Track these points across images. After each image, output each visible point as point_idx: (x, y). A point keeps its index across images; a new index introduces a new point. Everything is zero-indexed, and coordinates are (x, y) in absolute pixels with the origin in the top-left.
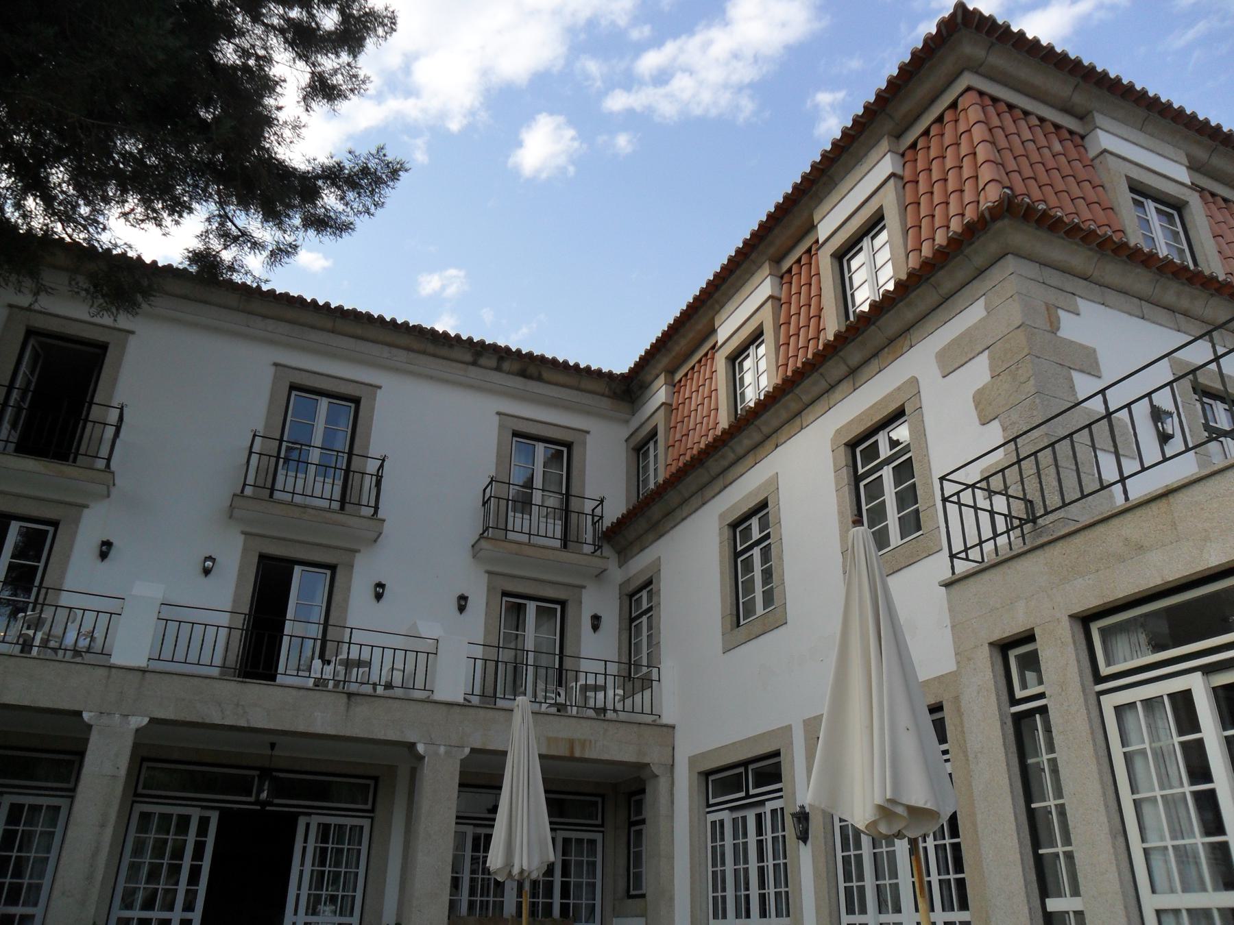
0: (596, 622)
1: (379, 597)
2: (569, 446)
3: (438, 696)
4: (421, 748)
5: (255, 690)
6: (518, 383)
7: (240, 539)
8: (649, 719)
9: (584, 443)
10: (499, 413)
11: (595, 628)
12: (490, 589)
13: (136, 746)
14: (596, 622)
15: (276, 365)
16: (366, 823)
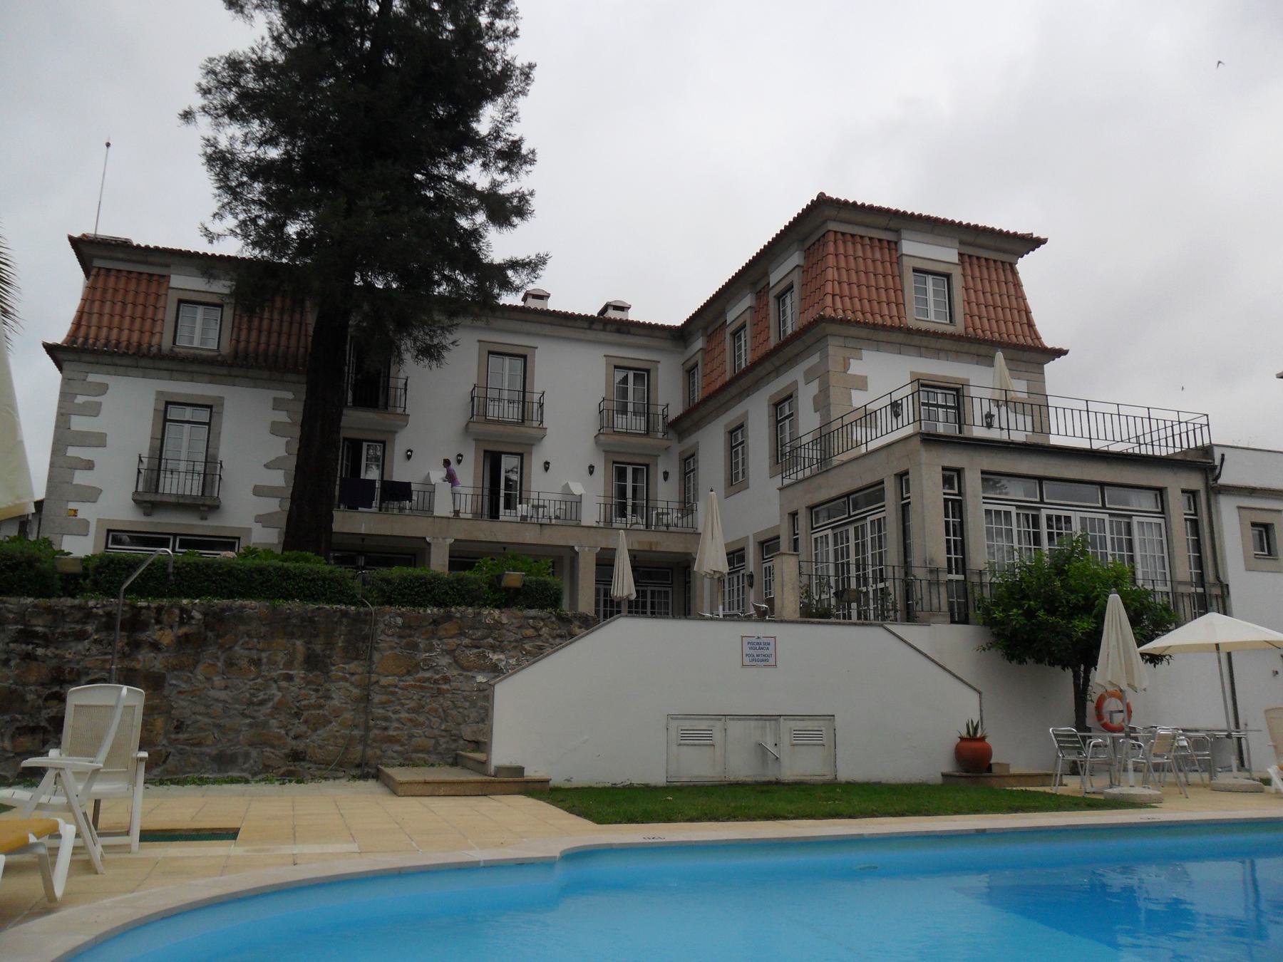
0: (666, 476)
1: (547, 469)
2: (648, 371)
3: (583, 523)
4: (576, 548)
5: (495, 525)
7: (474, 443)
8: (691, 530)
9: (657, 369)
10: (605, 356)
11: (666, 479)
14: (666, 476)
15: (479, 341)
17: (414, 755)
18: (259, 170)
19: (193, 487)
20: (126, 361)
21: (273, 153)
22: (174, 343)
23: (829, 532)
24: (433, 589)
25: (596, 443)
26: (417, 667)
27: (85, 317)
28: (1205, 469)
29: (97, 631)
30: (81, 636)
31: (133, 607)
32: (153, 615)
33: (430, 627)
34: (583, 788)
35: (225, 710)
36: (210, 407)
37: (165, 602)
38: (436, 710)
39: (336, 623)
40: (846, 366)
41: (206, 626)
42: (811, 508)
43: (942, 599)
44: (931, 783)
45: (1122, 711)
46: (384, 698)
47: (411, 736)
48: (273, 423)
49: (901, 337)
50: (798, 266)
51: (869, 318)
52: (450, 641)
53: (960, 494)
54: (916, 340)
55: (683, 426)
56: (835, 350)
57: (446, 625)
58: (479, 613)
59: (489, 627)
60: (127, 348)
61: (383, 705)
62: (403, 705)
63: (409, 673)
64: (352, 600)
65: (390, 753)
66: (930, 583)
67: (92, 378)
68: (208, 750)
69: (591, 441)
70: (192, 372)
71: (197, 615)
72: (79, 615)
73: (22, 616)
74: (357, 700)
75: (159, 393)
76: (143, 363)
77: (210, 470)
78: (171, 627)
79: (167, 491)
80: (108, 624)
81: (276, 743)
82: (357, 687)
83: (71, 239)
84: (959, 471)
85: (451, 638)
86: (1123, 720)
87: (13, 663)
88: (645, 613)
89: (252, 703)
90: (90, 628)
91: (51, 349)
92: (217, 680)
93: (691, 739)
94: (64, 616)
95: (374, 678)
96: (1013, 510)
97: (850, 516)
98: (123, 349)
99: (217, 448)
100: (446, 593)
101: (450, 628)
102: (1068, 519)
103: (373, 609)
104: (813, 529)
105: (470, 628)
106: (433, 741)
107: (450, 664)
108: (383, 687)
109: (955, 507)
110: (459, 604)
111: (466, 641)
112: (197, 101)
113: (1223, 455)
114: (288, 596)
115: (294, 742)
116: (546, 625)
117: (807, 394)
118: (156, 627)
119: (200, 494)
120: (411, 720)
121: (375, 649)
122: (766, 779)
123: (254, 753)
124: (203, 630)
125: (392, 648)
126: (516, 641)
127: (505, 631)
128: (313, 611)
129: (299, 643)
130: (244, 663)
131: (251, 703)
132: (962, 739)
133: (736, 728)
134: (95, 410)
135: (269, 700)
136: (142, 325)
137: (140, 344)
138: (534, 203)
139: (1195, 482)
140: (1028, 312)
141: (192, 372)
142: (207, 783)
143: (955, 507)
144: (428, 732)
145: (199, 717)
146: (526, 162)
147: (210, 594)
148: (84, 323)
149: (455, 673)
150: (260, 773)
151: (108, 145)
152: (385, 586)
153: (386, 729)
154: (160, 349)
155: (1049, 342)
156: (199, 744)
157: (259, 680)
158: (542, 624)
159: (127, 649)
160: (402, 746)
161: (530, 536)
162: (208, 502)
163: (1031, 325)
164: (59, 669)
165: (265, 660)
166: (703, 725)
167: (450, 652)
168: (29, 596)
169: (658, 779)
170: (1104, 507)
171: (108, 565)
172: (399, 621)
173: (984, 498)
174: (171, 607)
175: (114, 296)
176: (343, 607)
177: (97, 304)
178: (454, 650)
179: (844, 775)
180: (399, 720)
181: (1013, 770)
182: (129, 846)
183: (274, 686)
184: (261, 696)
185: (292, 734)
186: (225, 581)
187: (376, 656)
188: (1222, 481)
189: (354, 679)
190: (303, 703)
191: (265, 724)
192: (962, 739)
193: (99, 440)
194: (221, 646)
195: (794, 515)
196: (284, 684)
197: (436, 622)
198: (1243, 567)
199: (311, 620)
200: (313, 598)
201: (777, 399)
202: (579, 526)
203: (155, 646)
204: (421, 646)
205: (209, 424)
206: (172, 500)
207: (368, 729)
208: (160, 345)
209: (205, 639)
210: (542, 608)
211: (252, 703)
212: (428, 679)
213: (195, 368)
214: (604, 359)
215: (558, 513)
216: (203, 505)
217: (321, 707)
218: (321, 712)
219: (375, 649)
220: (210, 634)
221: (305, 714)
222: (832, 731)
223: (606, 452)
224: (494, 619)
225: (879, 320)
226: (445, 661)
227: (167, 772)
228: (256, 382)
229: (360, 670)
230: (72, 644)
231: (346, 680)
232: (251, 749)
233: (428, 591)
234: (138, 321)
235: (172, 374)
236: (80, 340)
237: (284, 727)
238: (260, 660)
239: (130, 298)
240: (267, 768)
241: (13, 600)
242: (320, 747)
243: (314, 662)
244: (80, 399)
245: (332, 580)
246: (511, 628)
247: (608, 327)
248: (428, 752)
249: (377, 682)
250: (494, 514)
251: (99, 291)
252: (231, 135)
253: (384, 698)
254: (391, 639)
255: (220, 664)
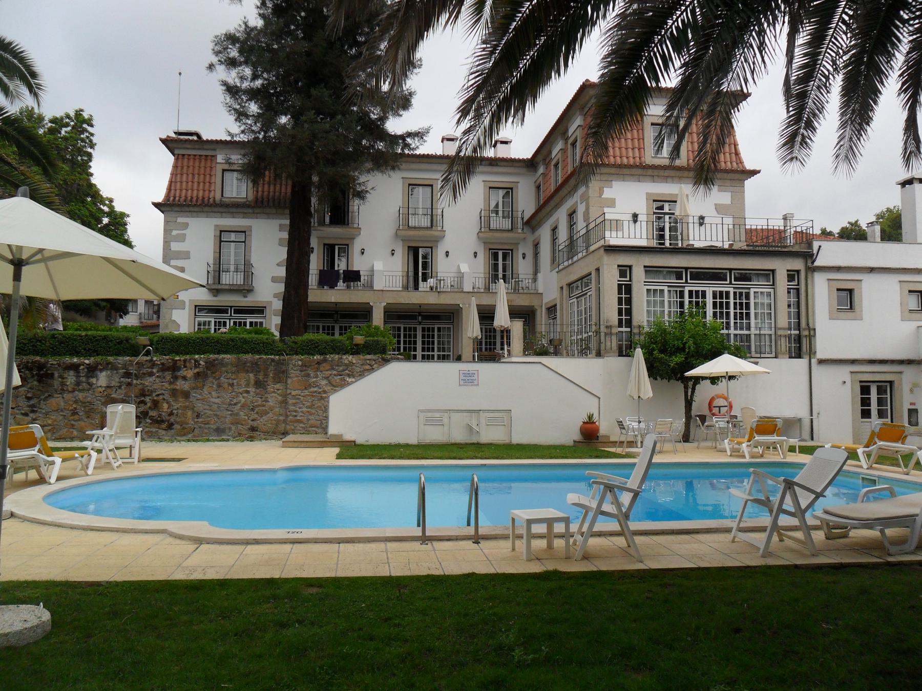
1: (447, 256)
2: (512, 189)
3: (465, 290)
4: (461, 306)
6: (489, 169)
7: (401, 242)
8: (535, 292)
9: (517, 187)
10: (483, 181)
11: (524, 258)
12: (485, 248)
13: (385, 312)
15: (403, 178)
16: (451, 326)
17: (310, 429)
18: (253, 94)
19: (238, 279)
20: (196, 209)
21: (258, 83)
22: (222, 196)
23: (575, 300)
24: (318, 346)
25: (478, 238)
26: (310, 386)
27: (173, 184)
28: (806, 257)
29: (158, 372)
30: (151, 374)
31: (173, 360)
32: (183, 363)
33: (316, 366)
34: (374, 445)
35: (219, 407)
36: (245, 232)
37: (188, 357)
38: (321, 407)
39: (269, 365)
40: (601, 192)
41: (207, 368)
42: (569, 285)
43: (614, 343)
44: (567, 445)
45: (726, 406)
46: (294, 401)
47: (308, 420)
48: (280, 239)
49: (639, 171)
50: (579, 126)
51: (619, 160)
52: (327, 372)
53: (630, 280)
54: (650, 172)
55: (532, 223)
56: (594, 184)
57: (324, 365)
58: (341, 358)
59: (346, 365)
60: (197, 201)
61: (294, 404)
62: (304, 404)
63: (306, 389)
64: (279, 353)
65: (298, 428)
66: (606, 334)
67: (180, 220)
68: (212, 426)
69: (476, 235)
70: (233, 213)
71: (202, 363)
72: (149, 365)
73: (125, 366)
74: (281, 402)
75: (216, 226)
76: (206, 209)
77: (247, 270)
78: (191, 369)
79: (224, 283)
80: (164, 368)
81: (244, 423)
82: (281, 396)
83: (161, 140)
84: (630, 267)
85: (327, 371)
86: (727, 412)
87: (123, 387)
88: (415, 357)
89: (231, 404)
90: (155, 370)
91: (157, 205)
92: (214, 394)
93: (430, 422)
94: (143, 365)
95: (289, 391)
96: (666, 289)
97: (582, 292)
98: (194, 202)
99: (250, 256)
100: (325, 348)
101: (325, 366)
102: (704, 293)
103: (286, 357)
104: (570, 297)
105: (338, 366)
106: (320, 422)
107: (327, 384)
108: (293, 396)
109: (626, 290)
110: (332, 354)
111: (335, 372)
112: (214, 59)
113: (820, 247)
114: (246, 352)
115: (252, 423)
116: (376, 363)
117: (581, 209)
118: (185, 369)
119: (242, 283)
120: (308, 412)
121: (289, 377)
122: (472, 442)
123: (233, 428)
124: (205, 370)
125: (297, 376)
126: (360, 372)
127: (354, 367)
128: (257, 359)
129: (251, 375)
130: (226, 385)
131: (230, 404)
132: (584, 423)
133: (456, 417)
134: (181, 239)
135: (239, 402)
136: (204, 186)
137: (203, 198)
138: (414, 101)
139: (797, 264)
140: (736, 145)
141: (233, 213)
142: (211, 441)
143: (626, 290)
144: (317, 418)
145: (207, 411)
146: (415, 67)
147: (209, 352)
148: (173, 188)
149: (329, 388)
150: (237, 437)
151: (180, 74)
152: (293, 345)
153: (296, 416)
154: (214, 201)
155: (749, 166)
156: (208, 424)
157: (234, 393)
158: (374, 362)
159: (172, 380)
160: (304, 424)
161: (432, 299)
162: (246, 288)
163: (737, 154)
164: (143, 390)
165: (235, 384)
166: (438, 415)
167: (327, 378)
168: (128, 356)
169: (413, 441)
170: (731, 283)
171: (161, 341)
172: (300, 363)
173: (645, 282)
174: (190, 359)
175: (187, 171)
176: (273, 357)
177: (179, 176)
178: (328, 377)
179: (516, 440)
180: (302, 412)
181: (612, 439)
182: (134, 462)
183: (241, 396)
184: (235, 401)
185: (251, 418)
186: (216, 346)
187: (289, 381)
188: (817, 264)
189: (279, 392)
190: (255, 404)
191: (237, 414)
192: (584, 423)
193: (186, 255)
194: (214, 378)
195: (562, 288)
196: (245, 395)
197: (319, 363)
198: (827, 316)
199: (256, 364)
200: (259, 353)
201: (570, 212)
202: (462, 292)
203: (184, 378)
204: (312, 375)
205: (244, 242)
206: (227, 287)
207: (287, 416)
208: (214, 198)
209: (207, 375)
210: (375, 354)
211: (231, 404)
212: (316, 392)
213: (234, 210)
214: (483, 183)
215: (452, 284)
216: (244, 290)
217: (264, 406)
218: (264, 408)
219: (289, 377)
220: (209, 372)
221: (257, 409)
222: (510, 418)
223: (484, 243)
224: (349, 361)
225: (625, 161)
226: (324, 382)
227: (194, 436)
228: (269, 216)
229: (281, 388)
230: (148, 378)
231: (274, 392)
232: (232, 426)
233: (316, 347)
234: (202, 184)
235: (222, 214)
236: (172, 198)
237: (247, 415)
238: (233, 384)
239: (196, 171)
240: (240, 434)
241: (121, 358)
242: (264, 425)
243: (258, 384)
244: (174, 233)
245: (267, 343)
246: (358, 365)
247: (484, 163)
248: (317, 427)
249: (290, 393)
250: (416, 287)
251: (179, 168)
252: (232, 77)
253: (294, 401)
254: (296, 372)
255: (214, 386)
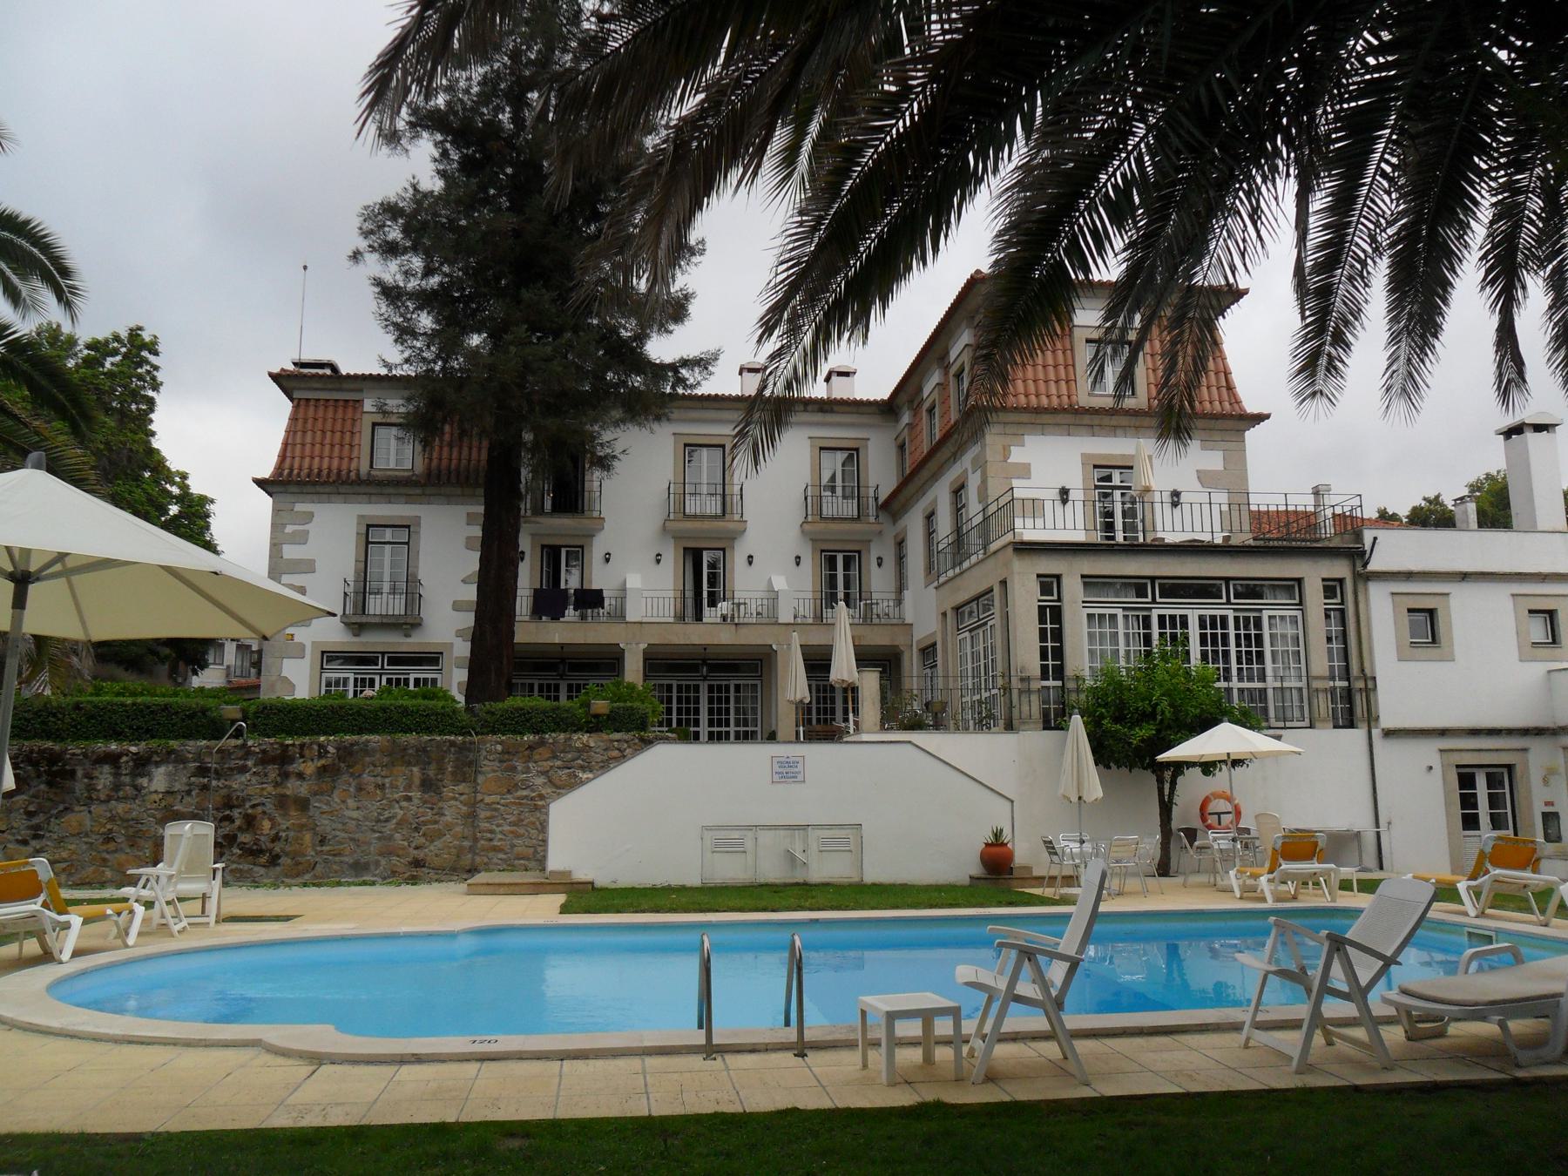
0: (880, 562)
1: (750, 563)
2: (857, 450)
3: (780, 621)
4: (774, 647)
6: (819, 417)
7: (672, 541)
8: (900, 622)
9: (866, 447)
11: (880, 565)
12: (814, 550)
13: (645, 660)
14: (880, 562)
15: (674, 434)
16: (759, 682)
18: (425, 299)
19: (397, 606)
20: (328, 489)
21: (434, 281)
22: (371, 467)
23: (967, 634)
24: (531, 718)
25: (803, 532)
27: (289, 448)
29: (255, 765)
30: (243, 770)
31: (282, 745)
32: (297, 750)
33: (527, 753)
35: (358, 826)
36: (408, 527)
37: (307, 739)
38: (534, 823)
39: (445, 752)
40: (1006, 457)
42: (957, 609)
44: (958, 884)
45: (1229, 813)
46: (488, 814)
47: (513, 846)
48: (468, 538)
50: (966, 345)
51: (1034, 401)
53: (1059, 599)
54: (1086, 419)
55: (893, 507)
59: (579, 750)
60: (329, 475)
61: (489, 819)
62: (505, 819)
63: (509, 792)
64: (463, 731)
65: (495, 860)
66: (1021, 692)
67: (299, 507)
70: (389, 494)
71: (330, 749)
72: (241, 753)
73: (198, 756)
75: (361, 517)
76: (342, 489)
77: (411, 590)
78: (312, 760)
79: (371, 612)
80: (265, 759)
81: (401, 852)
82: (465, 805)
83: (271, 375)
84: (1058, 577)
85: (546, 760)
86: (1231, 822)
87: (193, 793)
88: (696, 737)
90: (250, 763)
91: (261, 483)
92: (351, 803)
94: (230, 754)
95: (479, 797)
96: (1120, 613)
97: (979, 620)
98: (324, 478)
99: (417, 567)
100: (543, 721)
101: (543, 752)
102: (1184, 619)
103: (476, 738)
104: (959, 630)
106: (532, 850)
108: (488, 804)
109: (1051, 615)
110: (554, 731)
111: (559, 763)
112: (362, 244)
113: (1375, 539)
114: (407, 730)
115: (415, 852)
116: (629, 747)
117: (974, 482)
118: (302, 760)
119: (403, 613)
120: (512, 832)
122: (795, 881)
123: (383, 862)
124: (337, 761)
125: (494, 771)
126: (602, 761)
129: (415, 769)
130: (371, 788)
131: (378, 821)
132: (987, 845)
133: (766, 837)
134: (301, 538)
135: (393, 817)
136: (341, 451)
137: (339, 471)
138: (692, 308)
139: (1339, 569)
140: (1227, 373)
141: (389, 494)
143: (1051, 615)
145: (338, 833)
146: (693, 254)
148: (288, 454)
149: (549, 791)
150: (389, 877)
151: (305, 268)
152: (488, 718)
153: (491, 840)
154: (358, 474)
155: (1251, 407)
156: (339, 854)
157: (384, 802)
158: (626, 745)
159: (279, 779)
160: (506, 854)
161: (726, 637)
162: (409, 621)
163: (1230, 388)
164: (229, 797)
165: (387, 785)
166: (736, 835)
167: (545, 773)
168: (204, 739)
169: (694, 880)
170: (1228, 602)
171: (262, 712)
172: (499, 748)
173: (1083, 602)
174: (311, 744)
175: (313, 426)
177: (299, 434)
178: (548, 771)
179: (871, 876)
181: (1036, 873)
182: (208, 923)
183: (397, 806)
184: (387, 814)
185: (413, 845)
186: (356, 720)
187: (480, 779)
188: (1372, 567)
189: (462, 798)
190: (422, 819)
191: (390, 838)
192: (987, 845)
193: (307, 567)
194: (352, 775)
196: (404, 804)
197: (531, 748)
199: (424, 750)
200: (429, 731)
201: (956, 486)
202: (777, 624)
203: (300, 776)
204: (519, 768)
205: (408, 543)
206: (377, 620)
207: (476, 840)
208: (358, 470)
209: (338, 770)
210: (628, 731)
213: (391, 490)
215: (760, 609)
216: (406, 624)
217: (436, 822)
218: (436, 826)
220: (342, 765)
223: (812, 540)
225: (1045, 401)
226: (540, 780)
227: (316, 877)
228: (449, 499)
230: (237, 776)
231: (456, 799)
232: (380, 858)
233: (527, 721)
234: (337, 448)
235: (370, 497)
236: (286, 472)
238: (384, 785)
239: (329, 426)
240: (394, 873)
241: (191, 743)
242: (437, 855)
243: (427, 785)
244: (289, 529)
245: (443, 714)
247: (810, 408)
248: (528, 859)
249: (482, 800)
250: (699, 617)
251: (300, 422)
252: (391, 271)
254: (493, 763)
255: (352, 790)
